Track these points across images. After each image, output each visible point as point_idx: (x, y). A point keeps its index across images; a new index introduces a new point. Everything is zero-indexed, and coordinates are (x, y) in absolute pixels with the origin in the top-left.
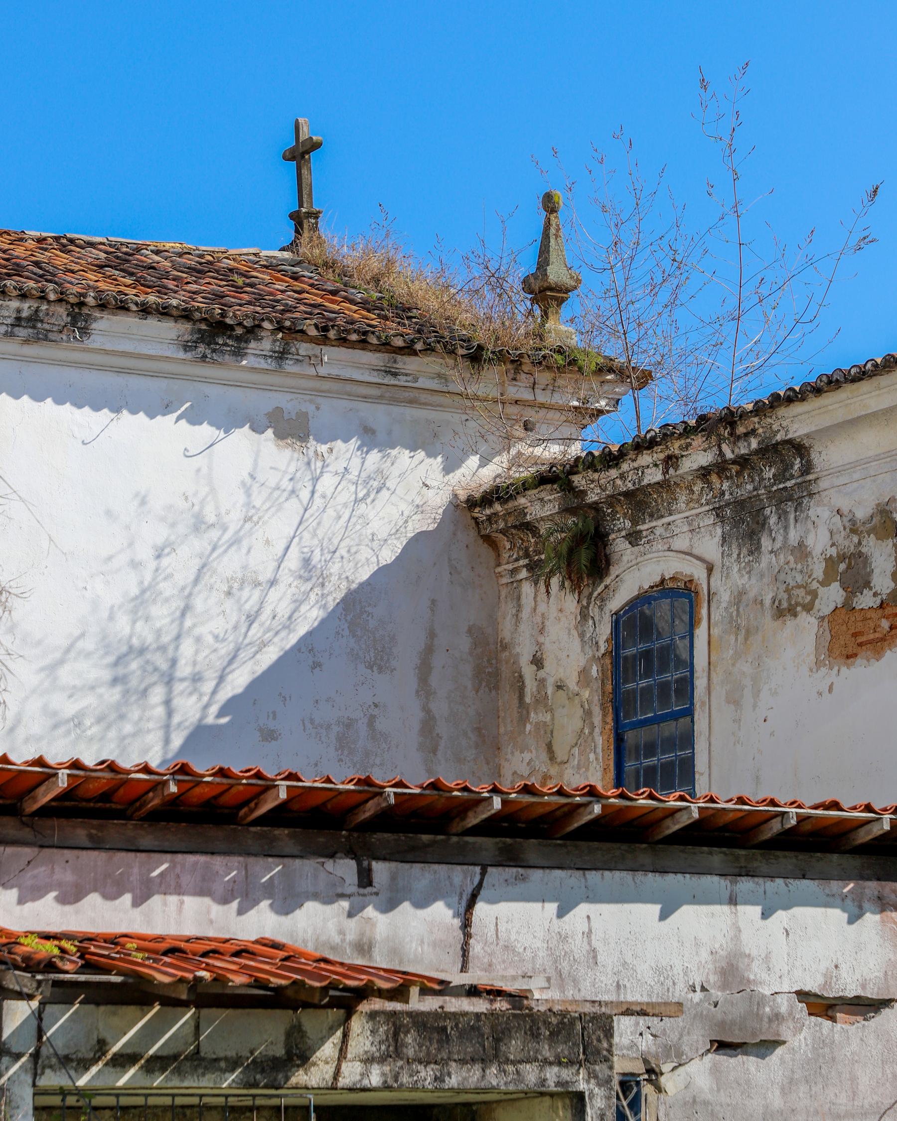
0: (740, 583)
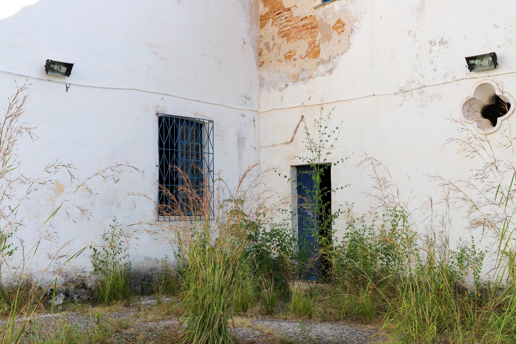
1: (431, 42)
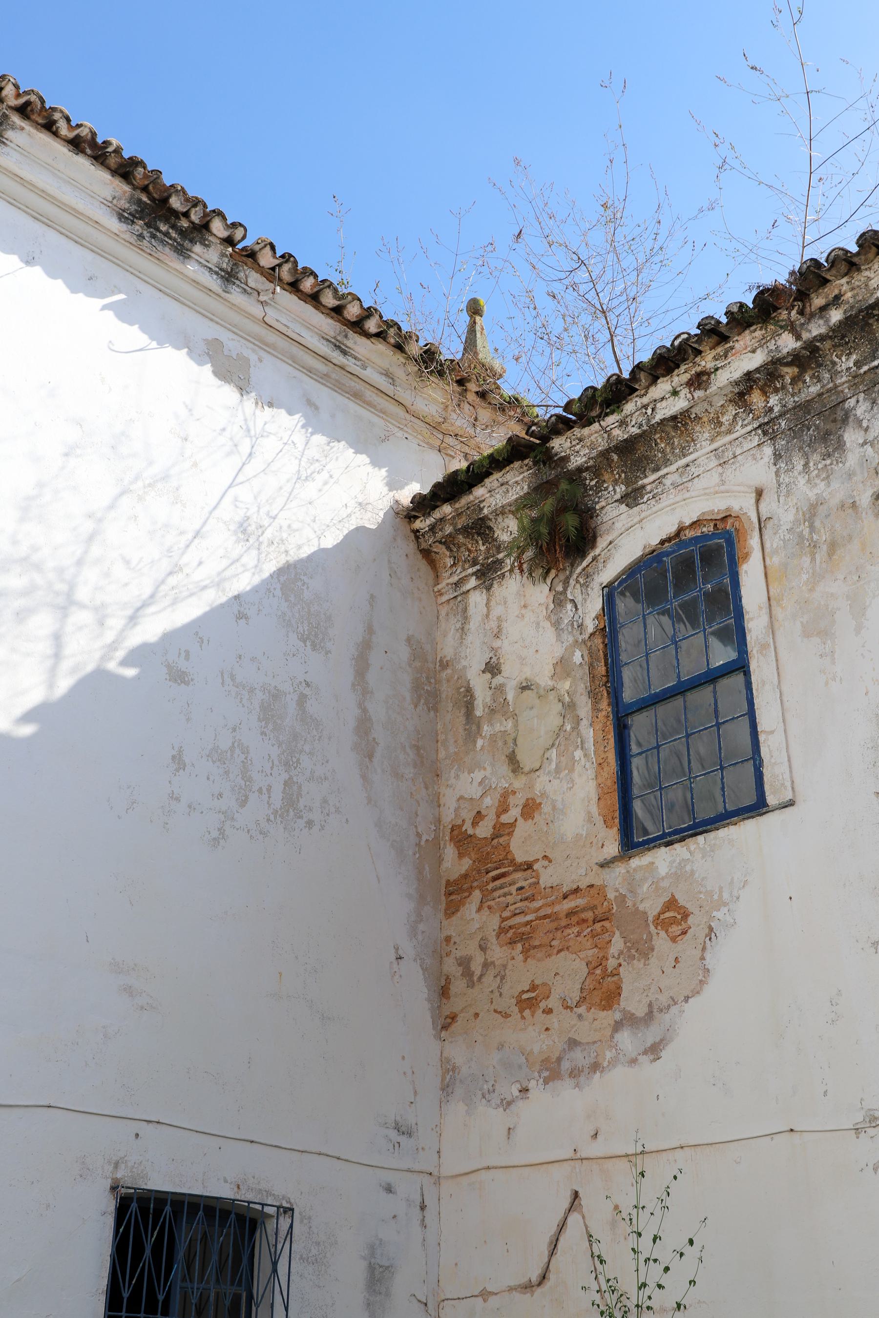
0: (812, 495)
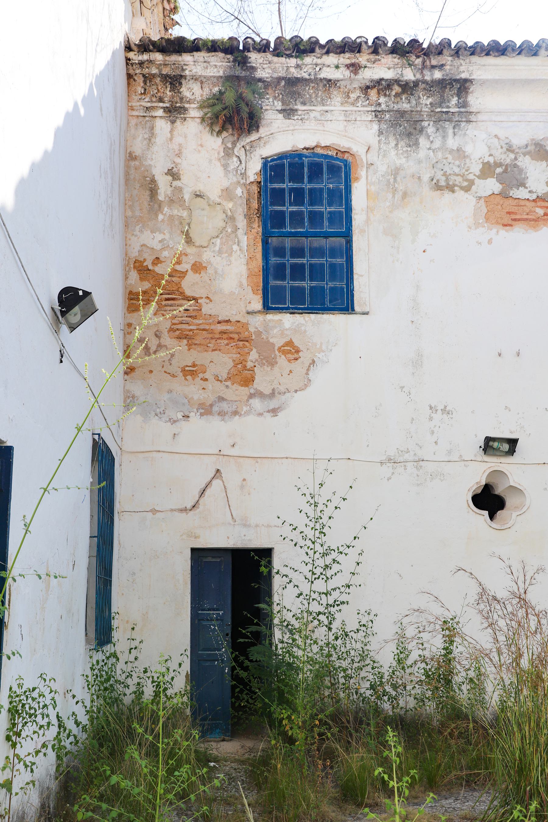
0: (398, 162)
1: (431, 408)
